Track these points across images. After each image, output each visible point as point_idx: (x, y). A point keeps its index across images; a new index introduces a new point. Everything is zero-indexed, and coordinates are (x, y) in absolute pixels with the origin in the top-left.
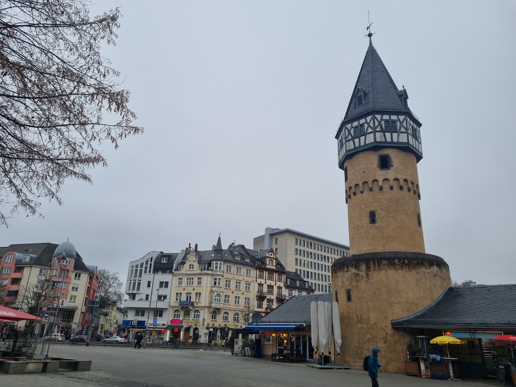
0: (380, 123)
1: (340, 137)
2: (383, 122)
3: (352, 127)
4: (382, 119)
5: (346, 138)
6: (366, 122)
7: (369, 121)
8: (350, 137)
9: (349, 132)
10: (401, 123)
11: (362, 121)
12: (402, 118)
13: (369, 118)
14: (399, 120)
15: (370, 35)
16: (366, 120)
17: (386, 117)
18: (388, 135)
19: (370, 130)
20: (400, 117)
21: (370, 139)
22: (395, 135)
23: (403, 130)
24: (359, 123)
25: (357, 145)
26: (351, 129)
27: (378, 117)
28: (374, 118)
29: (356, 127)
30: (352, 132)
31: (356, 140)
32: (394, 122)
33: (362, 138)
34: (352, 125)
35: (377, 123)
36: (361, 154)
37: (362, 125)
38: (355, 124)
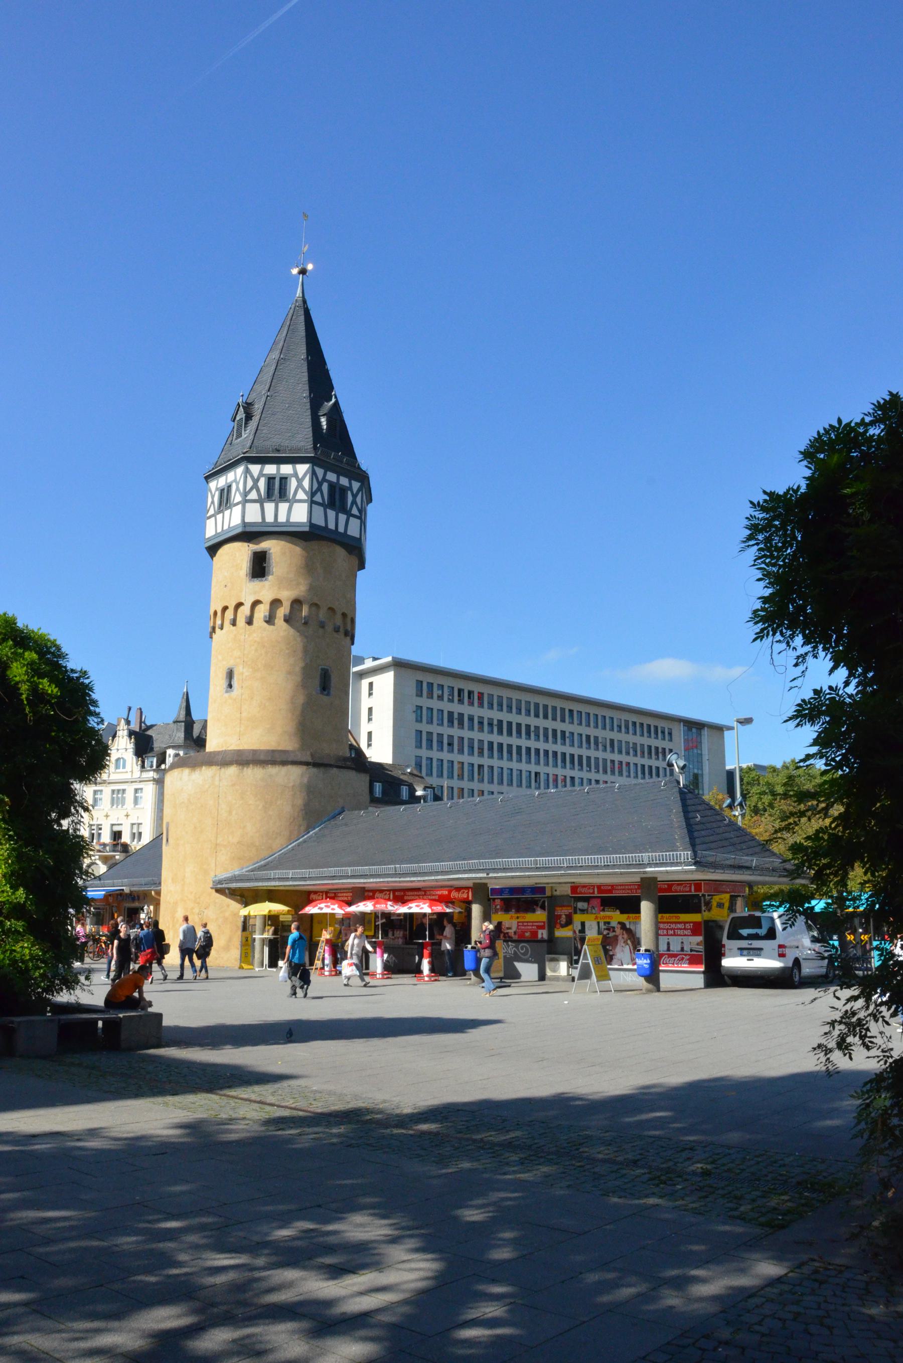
3: (261, 474)
5: (246, 494)
6: (295, 474)
9: (256, 481)
10: (355, 496)
11: (286, 469)
12: (356, 485)
14: (350, 488)
16: (295, 470)
17: (332, 477)
18: (331, 514)
20: (353, 482)
22: (342, 517)
23: (355, 511)
24: (278, 469)
25: (270, 518)
29: (270, 480)
30: (262, 484)
31: (269, 507)
32: (343, 490)
33: (283, 507)
34: (262, 470)
38: (271, 469)
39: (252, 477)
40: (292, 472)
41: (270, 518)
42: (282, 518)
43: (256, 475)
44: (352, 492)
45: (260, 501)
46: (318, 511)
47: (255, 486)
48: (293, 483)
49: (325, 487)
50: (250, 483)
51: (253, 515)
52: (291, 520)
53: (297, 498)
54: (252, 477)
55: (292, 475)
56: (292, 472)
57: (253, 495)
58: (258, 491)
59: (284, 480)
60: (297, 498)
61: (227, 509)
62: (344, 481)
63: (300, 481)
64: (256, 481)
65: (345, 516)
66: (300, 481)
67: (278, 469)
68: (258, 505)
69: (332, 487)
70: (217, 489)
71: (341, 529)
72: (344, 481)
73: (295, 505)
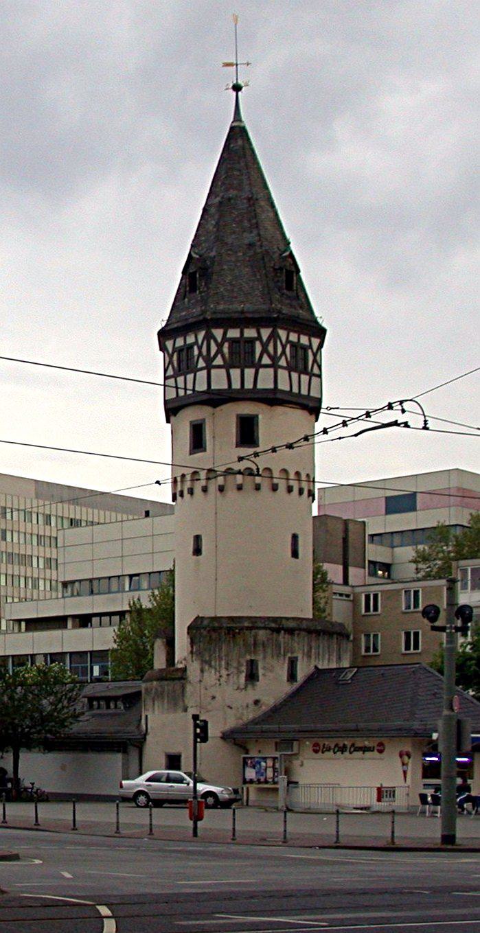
0: (284, 347)
1: (180, 342)
2: (288, 346)
4: (288, 341)
6: (259, 338)
7: (265, 339)
8: (219, 361)
11: (250, 333)
13: (265, 333)
15: (237, 88)
16: (259, 333)
17: (293, 337)
19: (266, 360)
20: (313, 339)
21: (265, 380)
22: (305, 378)
24: (242, 333)
25: (236, 385)
27: (282, 333)
28: (274, 336)
31: (235, 373)
32: (305, 349)
33: (250, 373)
34: (225, 334)
35: (280, 350)
37: (251, 341)
38: (234, 333)
39: (216, 341)
40: (256, 335)
41: (236, 385)
42: (249, 385)
43: (219, 340)
44: (312, 351)
45: (227, 366)
46: (283, 374)
47: (220, 351)
48: (258, 348)
50: (214, 349)
51: (219, 381)
52: (259, 386)
54: (216, 341)
55: (256, 339)
56: (256, 335)
62: (304, 340)
64: (220, 346)
65: (307, 377)
67: (242, 333)
68: (223, 371)
72: (304, 340)
73: (261, 370)
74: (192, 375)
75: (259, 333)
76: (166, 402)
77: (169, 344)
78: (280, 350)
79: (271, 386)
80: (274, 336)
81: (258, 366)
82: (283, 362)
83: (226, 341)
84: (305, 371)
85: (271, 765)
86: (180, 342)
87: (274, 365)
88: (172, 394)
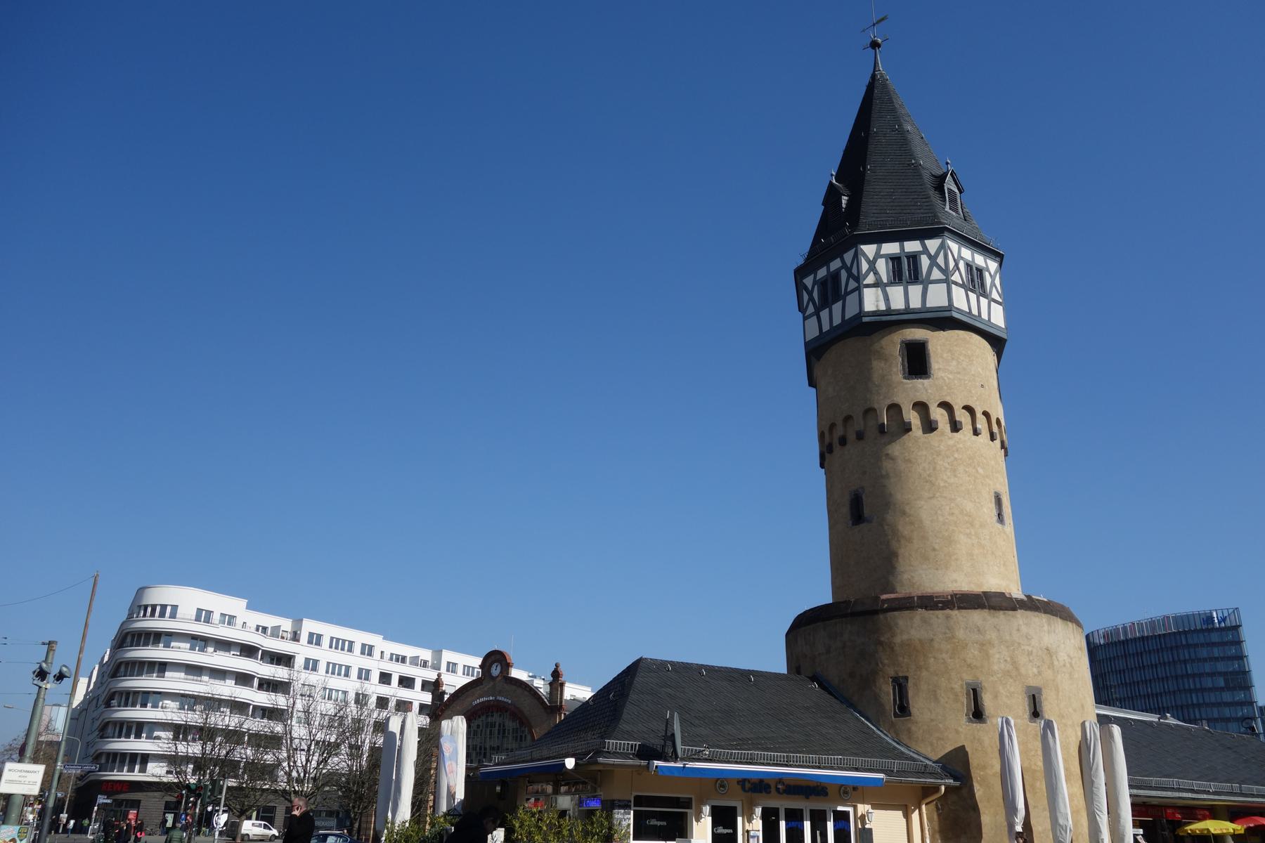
1: (822, 273)
6: (925, 250)
9: (872, 264)
11: (912, 246)
13: (933, 244)
16: (924, 246)
19: (936, 274)
21: (937, 297)
22: (984, 301)
23: (995, 295)
24: (902, 248)
26: (875, 259)
28: (943, 246)
29: (895, 260)
30: (882, 265)
33: (915, 291)
34: (879, 250)
35: (952, 264)
36: (976, 338)
38: (891, 248)
42: (915, 303)
48: (925, 262)
49: (962, 265)
52: (928, 305)
53: (932, 278)
57: (870, 279)
58: (876, 273)
59: (914, 258)
60: (932, 278)
61: (835, 301)
63: (933, 259)
66: (933, 259)
69: (969, 266)
70: (815, 282)
71: (985, 316)
74: (839, 304)
75: (924, 246)
76: (807, 344)
77: (808, 281)
78: (952, 264)
79: (946, 304)
80: (943, 246)
81: (926, 282)
82: (956, 277)
83: (882, 256)
84: (985, 296)
85: (1209, 679)
86: (822, 273)
87: (948, 282)
88: (813, 333)
